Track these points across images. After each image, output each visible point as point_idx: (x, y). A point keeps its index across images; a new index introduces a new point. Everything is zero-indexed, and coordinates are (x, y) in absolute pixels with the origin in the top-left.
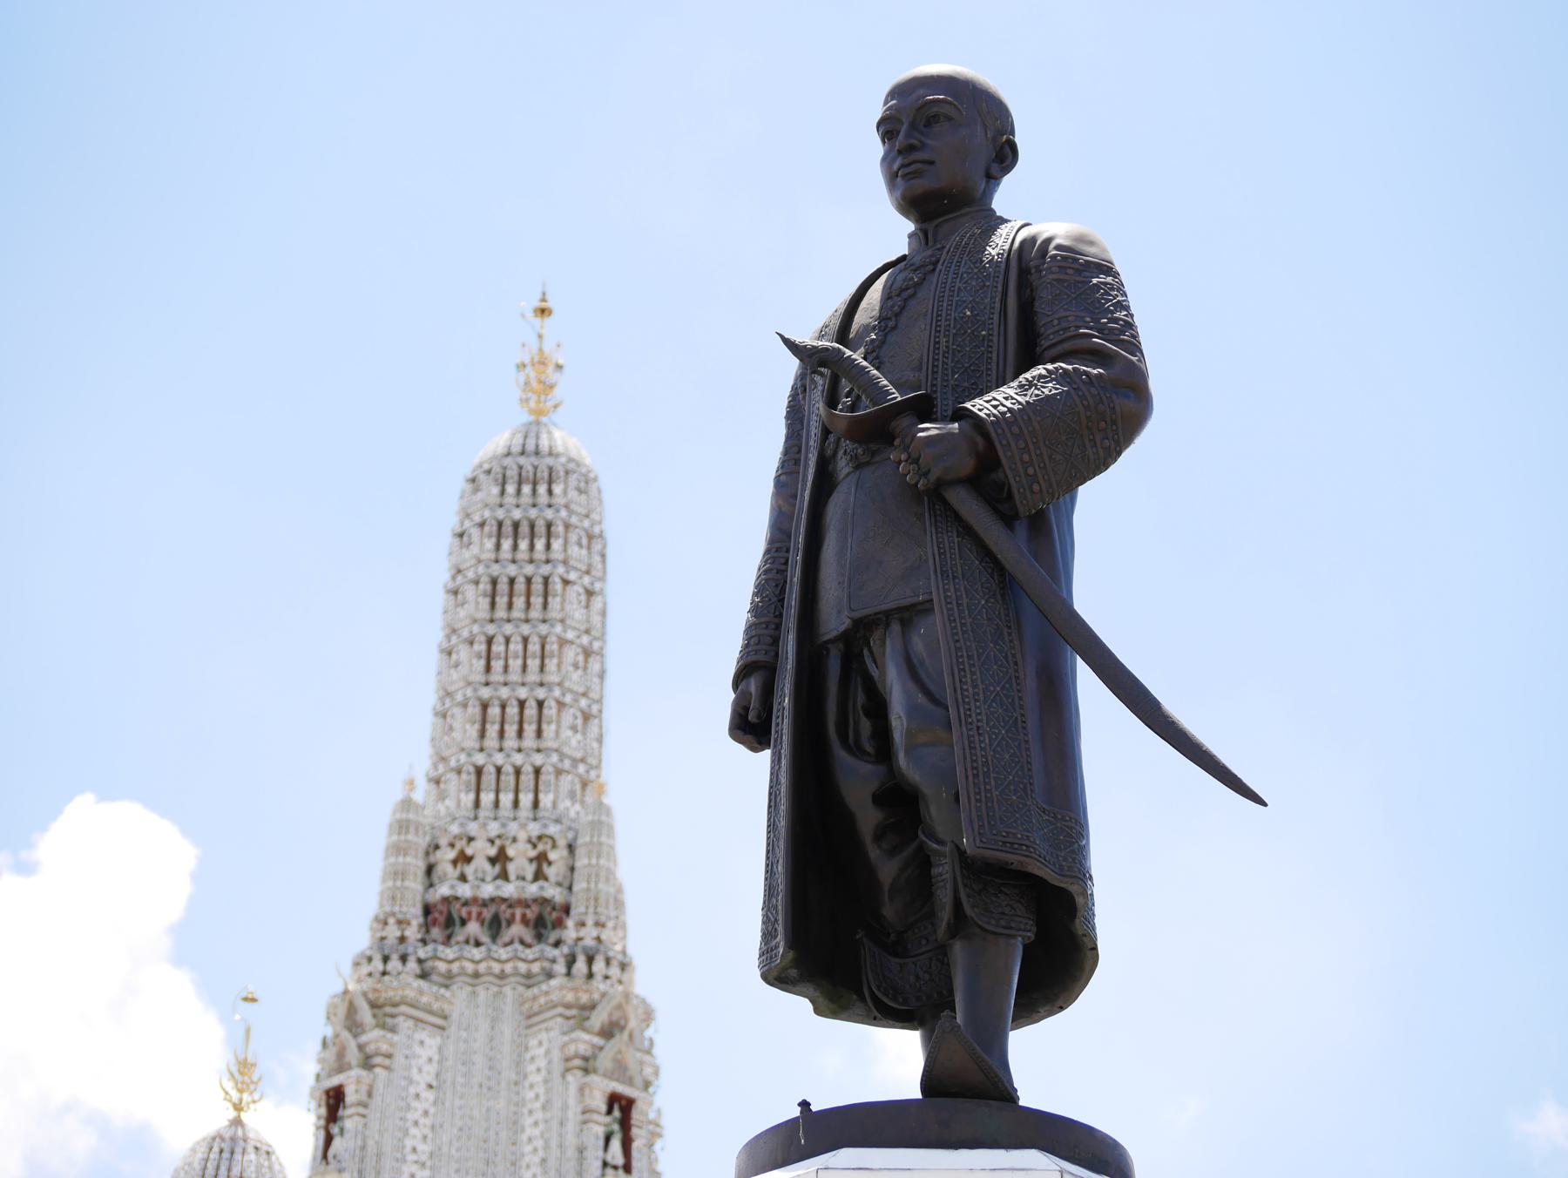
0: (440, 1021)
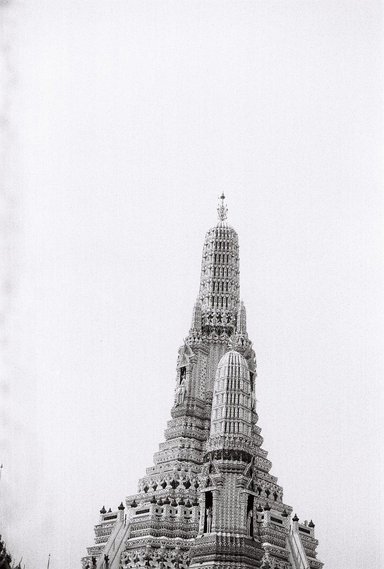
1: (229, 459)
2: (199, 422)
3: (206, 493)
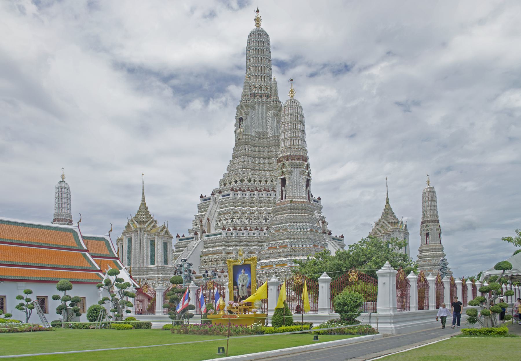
0: (254, 109)
1: (294, 160)
2: (253, 148)
3: (282, 179)
